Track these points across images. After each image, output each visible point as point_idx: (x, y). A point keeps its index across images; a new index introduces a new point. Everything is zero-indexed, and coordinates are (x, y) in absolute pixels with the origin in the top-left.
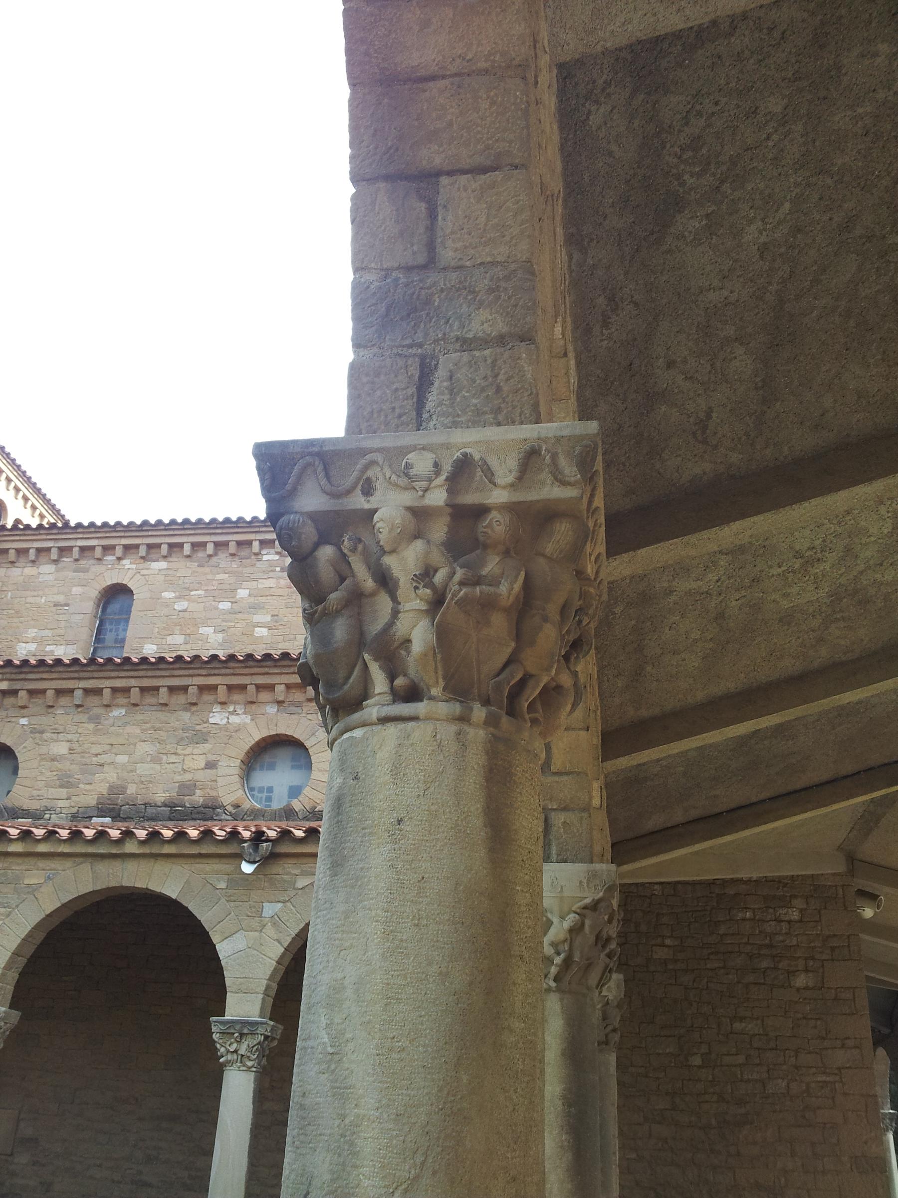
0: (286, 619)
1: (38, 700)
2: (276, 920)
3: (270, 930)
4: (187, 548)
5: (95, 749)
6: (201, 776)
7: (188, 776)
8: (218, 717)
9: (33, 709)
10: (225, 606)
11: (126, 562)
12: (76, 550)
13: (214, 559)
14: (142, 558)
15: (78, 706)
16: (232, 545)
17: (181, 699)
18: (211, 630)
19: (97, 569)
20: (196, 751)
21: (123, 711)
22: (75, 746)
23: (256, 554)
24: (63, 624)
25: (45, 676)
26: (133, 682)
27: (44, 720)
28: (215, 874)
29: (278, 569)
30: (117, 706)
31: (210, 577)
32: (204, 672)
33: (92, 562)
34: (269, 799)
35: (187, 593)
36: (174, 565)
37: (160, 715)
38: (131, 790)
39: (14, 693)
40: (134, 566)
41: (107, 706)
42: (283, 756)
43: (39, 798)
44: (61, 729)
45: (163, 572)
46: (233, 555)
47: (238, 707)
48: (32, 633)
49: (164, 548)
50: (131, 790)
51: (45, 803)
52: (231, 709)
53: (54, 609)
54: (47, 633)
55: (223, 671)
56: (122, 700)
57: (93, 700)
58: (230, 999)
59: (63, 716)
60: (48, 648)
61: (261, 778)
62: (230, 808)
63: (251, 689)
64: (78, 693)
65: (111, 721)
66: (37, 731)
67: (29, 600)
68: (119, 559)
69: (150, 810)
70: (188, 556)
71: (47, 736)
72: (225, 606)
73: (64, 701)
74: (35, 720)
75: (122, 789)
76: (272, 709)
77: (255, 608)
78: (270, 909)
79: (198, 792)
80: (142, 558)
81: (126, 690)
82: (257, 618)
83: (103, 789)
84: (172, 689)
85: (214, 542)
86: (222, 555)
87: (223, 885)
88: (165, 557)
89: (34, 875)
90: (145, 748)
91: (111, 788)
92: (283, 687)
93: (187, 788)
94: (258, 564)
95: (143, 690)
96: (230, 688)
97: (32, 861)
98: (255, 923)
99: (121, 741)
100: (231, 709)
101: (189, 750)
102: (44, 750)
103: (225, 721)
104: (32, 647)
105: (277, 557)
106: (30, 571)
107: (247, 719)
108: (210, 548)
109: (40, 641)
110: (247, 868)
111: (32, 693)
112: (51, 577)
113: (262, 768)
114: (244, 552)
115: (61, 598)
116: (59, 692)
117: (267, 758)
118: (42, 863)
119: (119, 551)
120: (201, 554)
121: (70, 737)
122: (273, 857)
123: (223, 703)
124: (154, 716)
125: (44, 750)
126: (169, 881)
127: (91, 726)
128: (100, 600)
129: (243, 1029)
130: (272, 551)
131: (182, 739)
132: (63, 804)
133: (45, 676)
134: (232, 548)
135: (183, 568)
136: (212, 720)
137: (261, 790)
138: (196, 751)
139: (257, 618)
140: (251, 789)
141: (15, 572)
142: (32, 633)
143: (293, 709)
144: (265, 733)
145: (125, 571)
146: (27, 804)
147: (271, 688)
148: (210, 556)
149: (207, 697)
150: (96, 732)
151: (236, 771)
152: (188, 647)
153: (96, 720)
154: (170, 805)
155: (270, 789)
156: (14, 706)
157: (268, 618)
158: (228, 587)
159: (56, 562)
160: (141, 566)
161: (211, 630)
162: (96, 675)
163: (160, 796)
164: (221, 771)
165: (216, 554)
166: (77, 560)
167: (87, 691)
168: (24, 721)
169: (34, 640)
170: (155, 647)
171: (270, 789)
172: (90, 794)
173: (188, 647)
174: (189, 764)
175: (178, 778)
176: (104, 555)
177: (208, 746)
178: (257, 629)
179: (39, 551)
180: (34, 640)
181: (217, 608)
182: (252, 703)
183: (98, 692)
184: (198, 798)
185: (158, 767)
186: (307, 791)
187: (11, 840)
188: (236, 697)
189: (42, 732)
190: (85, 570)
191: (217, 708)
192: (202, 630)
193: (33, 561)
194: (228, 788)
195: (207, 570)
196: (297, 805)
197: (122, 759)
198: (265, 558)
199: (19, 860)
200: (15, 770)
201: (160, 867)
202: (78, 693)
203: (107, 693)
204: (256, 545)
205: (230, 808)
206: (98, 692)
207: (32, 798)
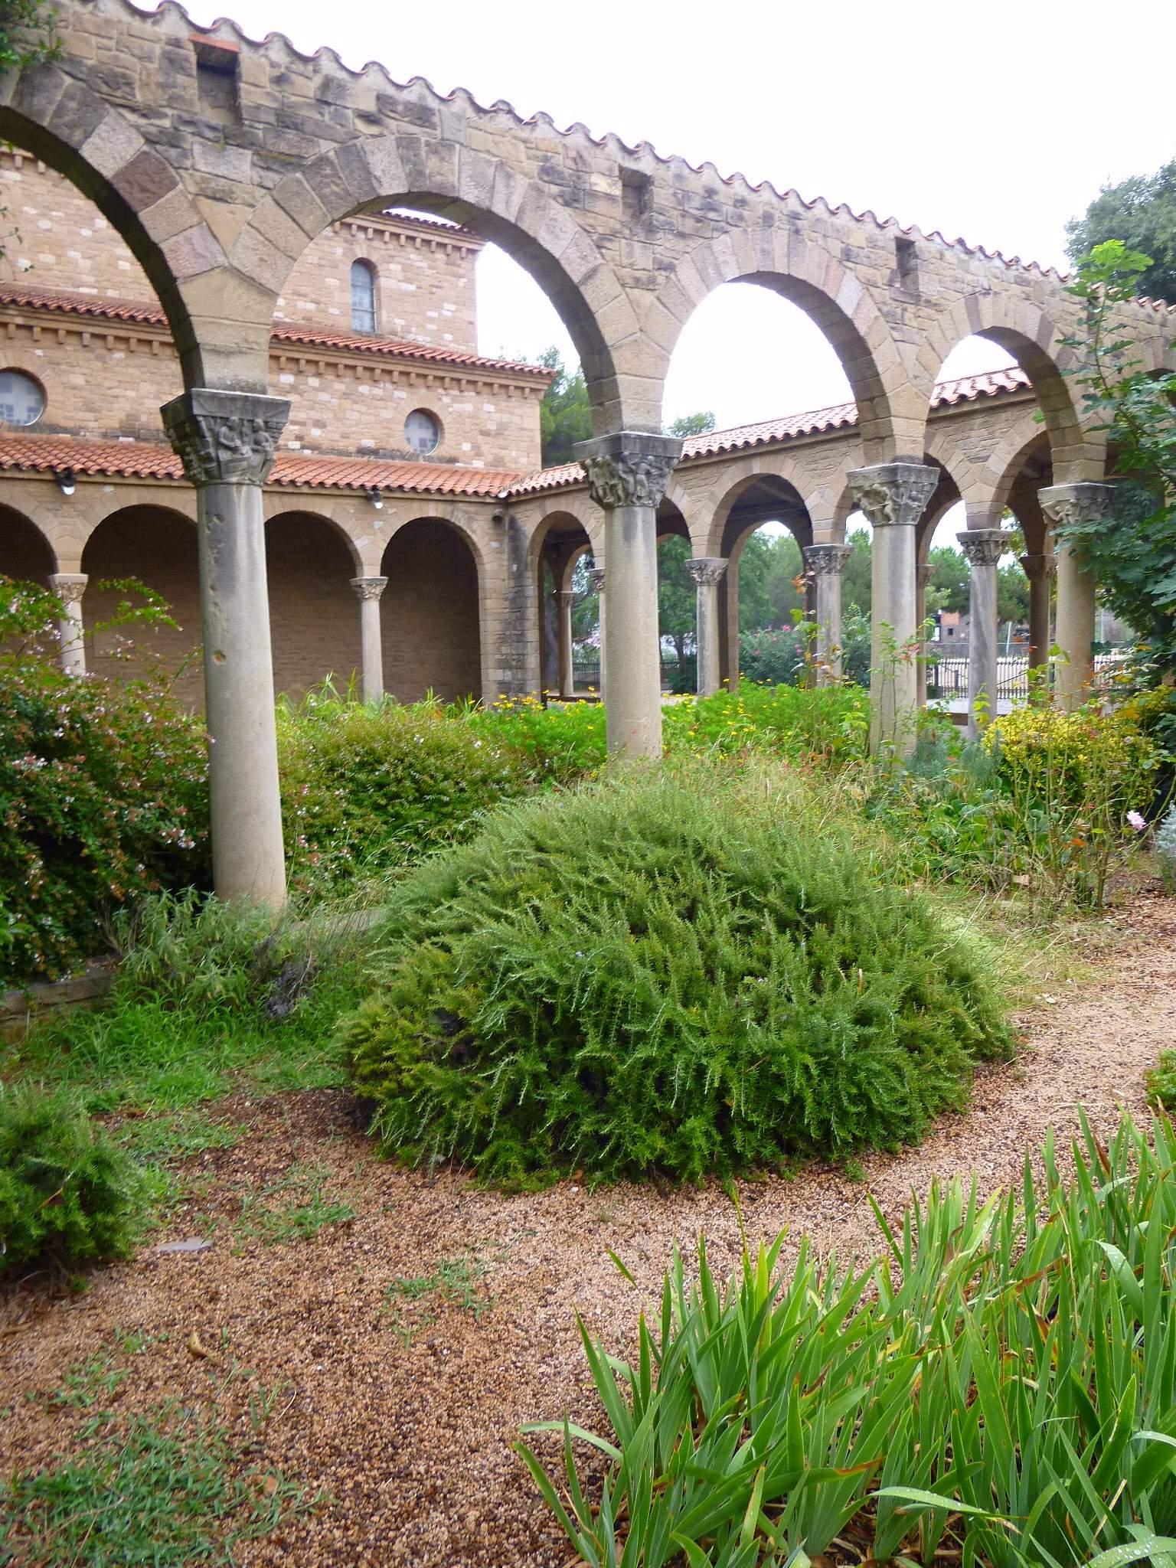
2: (382, 530)
3: (379, 535)
5: (107, 384)
10: (86, 232)
26: (131, 334)
27: (58, 354)
39: (30, 328)
43: (71, 418)
51: (78, 423)
57: (99, 343)
65: (114, 362)
66: (54, 363)
71: (63, 367)
74: (50, 353)
75: (137, 418)
78: (378, 524)
83: (122, 415)
91: (128, 416)
102: (65, 379)
125: (65, 379)
126: (325, 508)
127: (99, 364)
146: (63, 423)
150: (105, 369)
152: (60, 268)
153: (99, 358)
168: (39, 352)
181: (79, 234)
197: (131, 394)
201: (318, 501)
207: (65, 418)
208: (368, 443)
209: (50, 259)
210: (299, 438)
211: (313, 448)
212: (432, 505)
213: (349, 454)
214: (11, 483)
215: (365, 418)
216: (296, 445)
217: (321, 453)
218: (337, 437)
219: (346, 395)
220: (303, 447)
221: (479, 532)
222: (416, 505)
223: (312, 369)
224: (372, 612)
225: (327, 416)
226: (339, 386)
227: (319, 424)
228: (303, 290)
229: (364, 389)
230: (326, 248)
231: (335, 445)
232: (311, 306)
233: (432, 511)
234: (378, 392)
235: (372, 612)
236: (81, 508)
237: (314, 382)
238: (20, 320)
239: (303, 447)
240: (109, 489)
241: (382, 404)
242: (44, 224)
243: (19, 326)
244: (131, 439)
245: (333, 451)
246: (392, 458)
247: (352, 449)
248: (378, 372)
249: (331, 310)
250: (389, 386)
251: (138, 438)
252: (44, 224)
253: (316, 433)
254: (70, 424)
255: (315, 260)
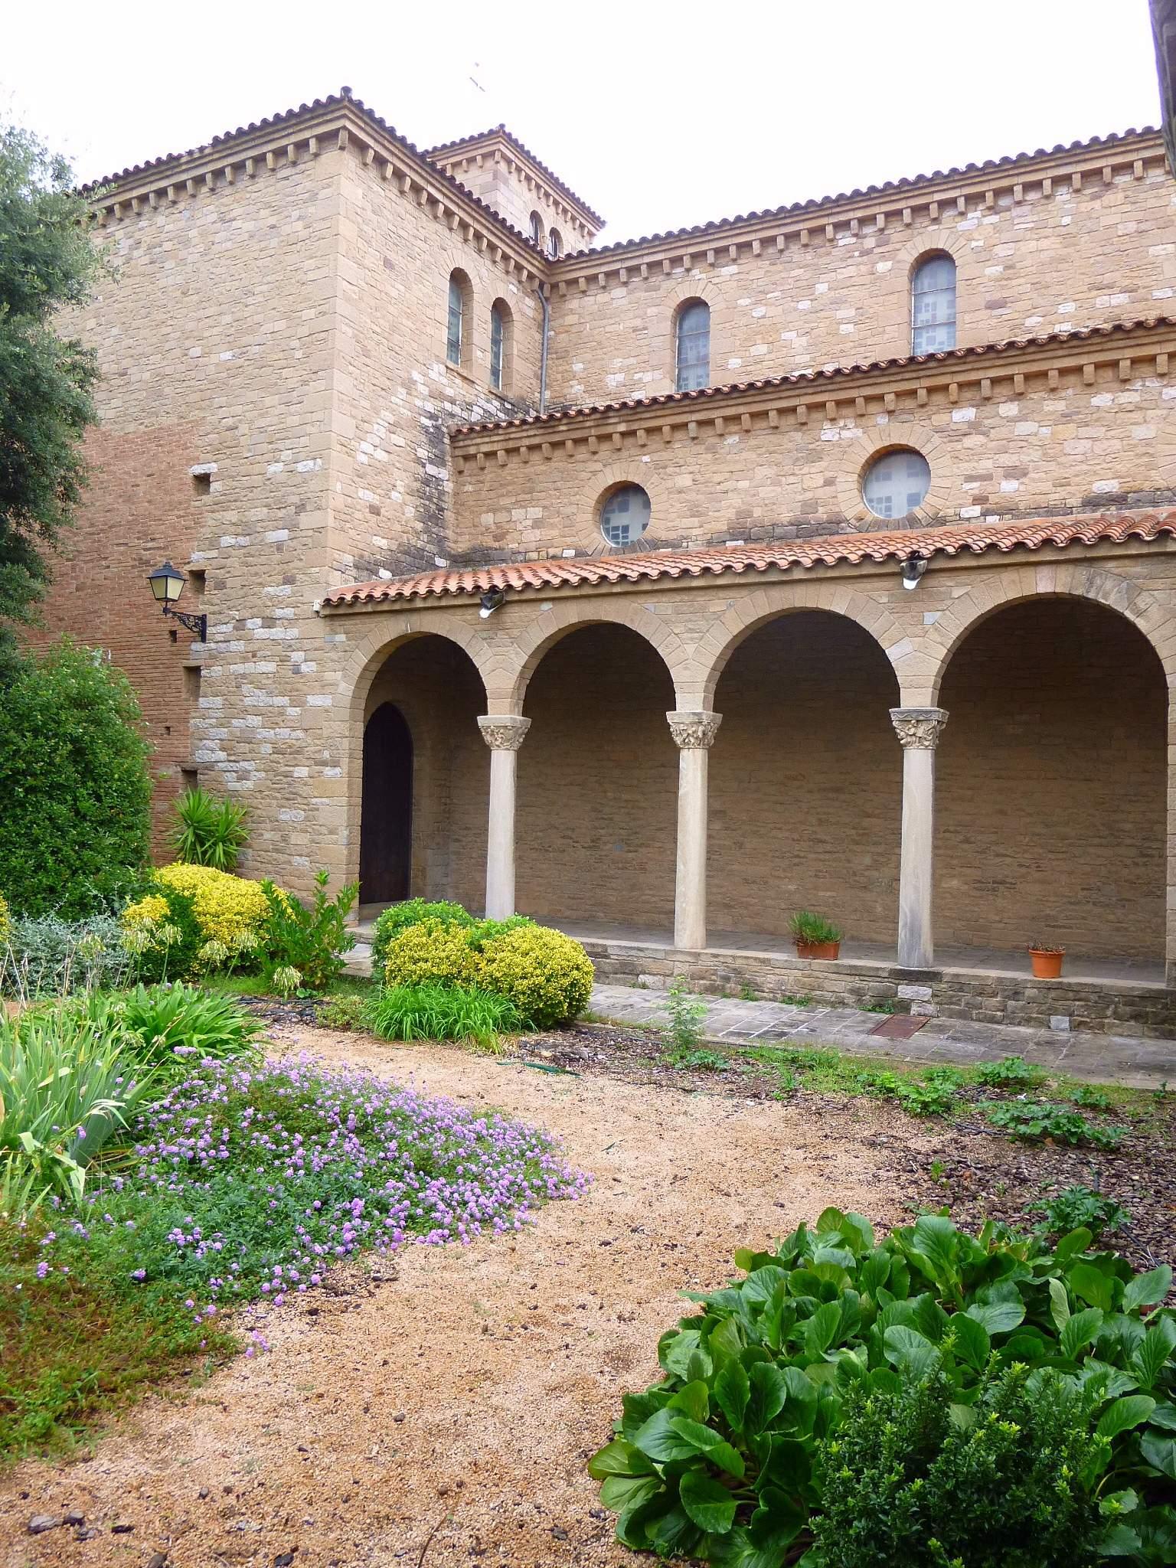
0: (871, 311)
1: (656, 437)
2: (937, 627)
4: (756, 245)
5: (717, 478)
6: (820, 493)
7: (809, 495)
8: (829, 433)
9: (652, 447)
10: (805, 305)
11: (695, 272)
12: (644, 268)
13: (786, 253)
14: (712, 265)
15: (694, 439)
16: (804, 234)
17: (791, 420)
18: (794, 334)
19: (668, 284)
20: (813, 470)
21: (736, 438)
22: (698, 477)
23: (831, 241)
24: (645, 349)
25: (659, 413)
26: (741, 409)
27: (665, 455)
28: (880, 592)
29: (857, 254)
30: (730, 433)
31: (783, 275)
32: (810, 391)
33: (662, 277)
34: (888, 509)
35: (762, 296)
36: (745, 268)
37: (772, 438)
38: (757, 513)
39: (632, 433)
40: (703, 276)
41: (721, 435)
42: (899, 463)
44: (682, 462)
45: (737, 277)
46: (806, 246)
47: (848, 421)
48: (617, 363)
49: (733, 250)
50: (757, 513)
51: (681, 532)
52: (842, 424)
53: (633, 335)
54: (632, 361)
55: (830, 387)
56: (734, 428)
57: (708, 431)
58: (904, 694)
59: (681, 449)
60: (637, 376)
61: (879, 489)
62: (853, 521)
63: (860, 401)
64: (692, 426)
65: (727, 449)
66: (659, 466)
67: (608, 329)
68: (688, 270)
69: (778, 531)
70: (759, 255)
71: (670, 470)
72: (805, 305)
73: (679, 435)
74: (656, 457)
75: (750, 514)
76: (883, 420)
77: (837, 303)
78: (930, 618)
79: (821, 509)
80: (712, 265)
81: (737, 418)
82: (840, 314)
83: (731, 514)
84: (781, 412)
85: (785, 235)
86: (794, 248)
87: (885, 600)
88: (734, 260)
89: (717, 604)
90: (762, 472)
92: (892, 396)
93: (810, 506)
94: (835, 252)
95: (753, 415)
96: (839, 403)
97: (713, 593)
98: (918, 630)
99: (739, 467)
100: (842, 424)
101: (806, 470)
102: (669, 484)
103: (837, 437)
104: (620, 377)
105: (854, 240)
106: (603, 298)
107: (859, 432)
108: (781, 240)
109: (626, 370)
110: (910, 585)
111: (649, 431)
112: (624, 301)
113: (877, 479)
114: (818, 240)
115: (638, 322)
116: (675, 427)
117: (882, 469)
118: (722, 594)
119: (687, 261)
120: (771, 250)
121: (691, 469)
122: (929, 572)
123: (833, 420)
124: (762, 438)
125: (669, 484)
126: (838, 601)
128: (675, 317)
129: (918, 717)
130: (848, 233)
131: (797, 459)
132: (696, 531)
133: (659, 413)
134: (804, 238)
135: (754, 269)
136: (823, 438)
137: (880, 500)
138: (813, 470)
139: (840, 314)
140: (870, 501)
141: (589, 300)
142: (617, 363)
143: (905, 417)
144: (879, 445)
145: (696, 283)
146: (664, 535)
147: (880, 398)
148: (781, 251)
149: (817, 415)
151: (855, 485)
152: (772, 356)
154: (796, 524)
155: (889, 499)
156: (634, 446)
157: (852, 312)
158: (805, 283)
159: (625, 284)
160: (711, 274)
161: (794, 334)
162: (706, 406)
163: (786, 516)
164: (840, 487)
165: (787, 247)
166: (646, 279)
167: (701, 423)
168: (646, 459)
169: (621, 370)
170: (739, 361)
171: (889, 499)
172: (720, 519)
173: (772, 356)
174: (808, 483)
175: (801, 498)
176: (672, 268)
177: (823, 464)
178: (843, 327)
179: (608, 274)
180: (621, 370)
181: (796, 309)
182: (862, 415)
183: (710, 422)
184: (822, 514)
185: (779, 489)
186: (929, 498)
187: (694, 577)
188: (845, 411)
189: (665, 468)
190: (657, 289)
191: (827, 425)
192: (786, 335)
193: (604, 287)
194: (849, 502)
195: (780, 267)
196: (919, 512)
197: (744, 484)
198: (841, 243)
199: (701, 593)
200: (647, 504)
201: (825, 589)
202: (692, 426)
203: (719, 422)
204: (829, 229)
205: (853, 521)
206: (710, 422)
207: (668, 529)
208: (1111, 486)
209: (762, 349)
210: (978, 500)
211: (1000, 513)
212: (1045, 572)
213: (1068, 511)
214: (451, 611)
215: (1099, 448)
216: (977, 510)
217: (1018, 517)
218: (1047, 487)
219: (1066, 417)
220: (985, 514)
221: (1155, 613)
222: (1008, 576)
223: (1004, 390)
224: (918, 768)
225: (1029, 457)
226: (1055, 406)
227: (1015, 472)
228: (1107, 279)
229: (1102, 400)
230: (1152, 203)
231: (1042, 500)
232: (1121, 299)
233: (1044, 583)
234: (1127, 398)
235: (918, 768)
236: (516, 632)
237: (1010, 409)
238: (622, 428)
239: (985, 514)
240: (546, 606)
241: (1137, 416)
242: (759, 311)
243: (623, 434)
244: (741, 543)
245: (1037, 510)
246: (1155, 503)
247: (1075, 501)
248: (1125, 364)
249: (1158, 294)
250: (1153, 384)
251: (748, 540)
252: (759, 311)
253: (1009, 486)
254: (672, 536)
255: (1132, 227)
